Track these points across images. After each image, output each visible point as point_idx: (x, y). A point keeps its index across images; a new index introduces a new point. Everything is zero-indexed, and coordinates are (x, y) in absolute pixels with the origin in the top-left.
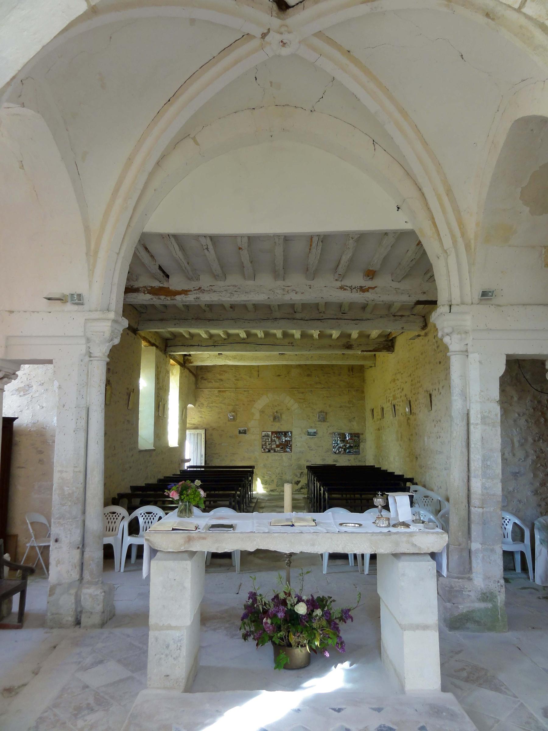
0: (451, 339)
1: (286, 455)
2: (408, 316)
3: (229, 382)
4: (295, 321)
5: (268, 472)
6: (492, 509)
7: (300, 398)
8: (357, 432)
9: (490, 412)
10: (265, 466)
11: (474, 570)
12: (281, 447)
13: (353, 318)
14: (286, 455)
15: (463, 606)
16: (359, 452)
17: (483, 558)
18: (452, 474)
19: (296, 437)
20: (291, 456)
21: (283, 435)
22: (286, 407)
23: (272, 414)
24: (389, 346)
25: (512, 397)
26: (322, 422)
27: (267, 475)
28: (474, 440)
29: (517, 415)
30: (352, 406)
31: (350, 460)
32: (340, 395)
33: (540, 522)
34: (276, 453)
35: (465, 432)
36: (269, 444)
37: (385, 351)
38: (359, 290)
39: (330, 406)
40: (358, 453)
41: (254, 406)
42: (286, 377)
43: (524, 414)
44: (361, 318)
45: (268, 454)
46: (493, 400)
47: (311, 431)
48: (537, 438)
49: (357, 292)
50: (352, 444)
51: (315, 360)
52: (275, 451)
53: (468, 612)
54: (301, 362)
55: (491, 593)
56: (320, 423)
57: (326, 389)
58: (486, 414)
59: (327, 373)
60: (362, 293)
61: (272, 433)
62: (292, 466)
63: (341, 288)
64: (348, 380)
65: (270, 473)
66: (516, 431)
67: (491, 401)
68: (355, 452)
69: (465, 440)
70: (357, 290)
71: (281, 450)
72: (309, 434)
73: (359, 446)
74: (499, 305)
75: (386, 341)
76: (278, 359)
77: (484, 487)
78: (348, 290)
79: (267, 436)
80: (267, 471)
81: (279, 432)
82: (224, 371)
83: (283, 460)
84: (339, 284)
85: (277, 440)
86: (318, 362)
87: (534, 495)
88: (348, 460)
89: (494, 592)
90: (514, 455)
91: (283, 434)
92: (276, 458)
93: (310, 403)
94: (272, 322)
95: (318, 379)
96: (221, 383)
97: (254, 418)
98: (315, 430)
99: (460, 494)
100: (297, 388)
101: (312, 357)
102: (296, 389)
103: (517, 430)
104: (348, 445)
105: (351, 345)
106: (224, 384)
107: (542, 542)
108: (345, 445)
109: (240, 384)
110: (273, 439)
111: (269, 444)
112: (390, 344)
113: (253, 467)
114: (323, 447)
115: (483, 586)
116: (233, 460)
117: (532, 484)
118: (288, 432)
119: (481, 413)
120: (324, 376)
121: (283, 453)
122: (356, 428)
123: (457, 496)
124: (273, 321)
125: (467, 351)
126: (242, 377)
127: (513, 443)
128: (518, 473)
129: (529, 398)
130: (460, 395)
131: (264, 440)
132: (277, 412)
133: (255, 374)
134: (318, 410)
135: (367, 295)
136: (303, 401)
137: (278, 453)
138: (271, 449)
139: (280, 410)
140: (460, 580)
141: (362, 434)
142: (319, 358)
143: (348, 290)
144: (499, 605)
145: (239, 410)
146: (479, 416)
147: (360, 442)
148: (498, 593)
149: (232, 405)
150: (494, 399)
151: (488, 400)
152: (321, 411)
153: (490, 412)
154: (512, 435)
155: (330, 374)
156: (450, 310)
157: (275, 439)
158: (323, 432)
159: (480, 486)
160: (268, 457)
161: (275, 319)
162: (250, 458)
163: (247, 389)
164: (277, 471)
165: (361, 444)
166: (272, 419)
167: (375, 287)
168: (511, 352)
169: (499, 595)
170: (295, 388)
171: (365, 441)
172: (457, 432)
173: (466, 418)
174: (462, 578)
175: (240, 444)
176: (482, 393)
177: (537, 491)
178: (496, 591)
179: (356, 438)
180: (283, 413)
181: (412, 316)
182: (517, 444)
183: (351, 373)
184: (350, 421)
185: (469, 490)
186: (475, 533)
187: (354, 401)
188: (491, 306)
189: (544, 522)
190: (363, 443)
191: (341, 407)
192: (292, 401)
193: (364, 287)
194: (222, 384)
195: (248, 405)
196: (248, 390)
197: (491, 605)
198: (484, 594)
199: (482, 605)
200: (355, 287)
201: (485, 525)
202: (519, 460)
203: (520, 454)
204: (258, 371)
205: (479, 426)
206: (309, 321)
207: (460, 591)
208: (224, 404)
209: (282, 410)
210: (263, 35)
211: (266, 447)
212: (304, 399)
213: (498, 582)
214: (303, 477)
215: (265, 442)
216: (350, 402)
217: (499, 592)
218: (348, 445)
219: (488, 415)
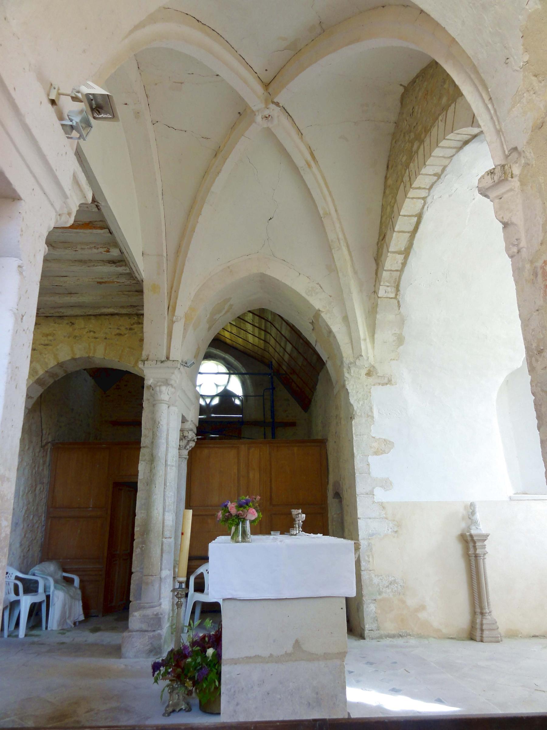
18: (157, 509)
28: (170, 479)
186: (165, 561)
210: (277, 103)
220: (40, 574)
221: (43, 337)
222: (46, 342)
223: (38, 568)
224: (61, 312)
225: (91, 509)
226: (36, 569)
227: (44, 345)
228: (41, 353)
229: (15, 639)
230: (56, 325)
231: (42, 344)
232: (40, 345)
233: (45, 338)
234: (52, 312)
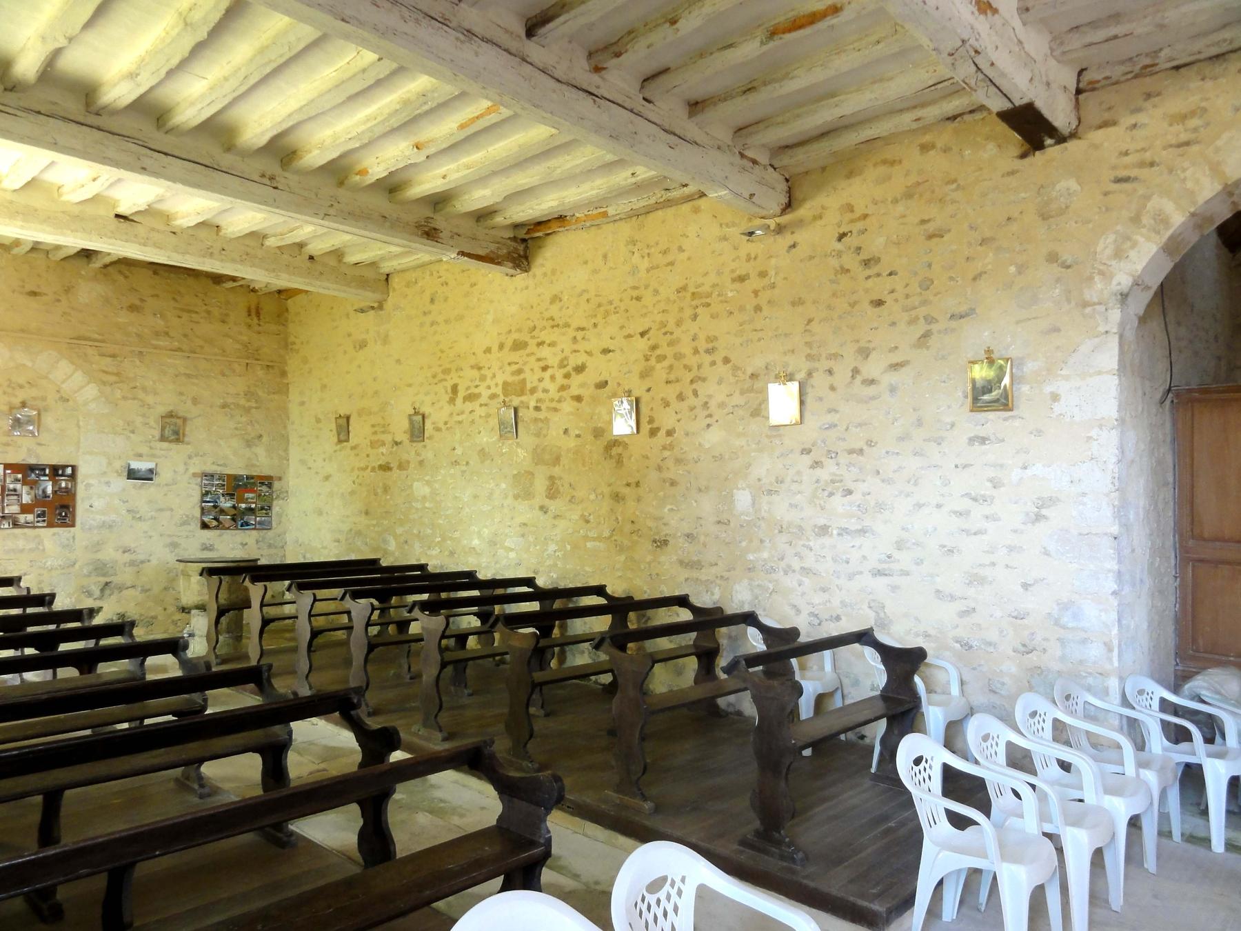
1: (54, 534)
2: (765, 167)
8: (266, 472)
12: (38, 510)
14: (54, 534)
16: (270, 523)
19: (91, 481)
20: (74, 538)
21: (45, 475)
22: (58, 391)
24: (520, 256)
26: (171, 442)
30: (254, 405)
31: (246, 544)
32: (223, 375)
34: (17, 531)
37: (511, 265)
39: (195, 401)
40: (265, 526)
42: (59, 301)
47: (141, 465)
50: (253, 503)
51: (234, 261)
52: (16, 524)
54: (188, 257)
56: (165, 445)
57: (184, 354)
59: (189, 311)
62: (77, 566)
64: (245, 338)
68: (260, 523)
71: (38, 522)
72: (132, 474)
73: (270, 508)
75: (514, 239)
76: (112, 232)
81: (32, 468)
83: (44, 550)
86: (239, 266)
88: (242, 544)
91: (47, 471)
92: (21, 543)
94: (457, 39)
95: (162, 323)
98: (151, 465)
101: (223, 250)
102: (91, 343)
104: (243, 506)
105: (435, 229)
108: (234, 507)
110: (11, 486)
112: (521, 248)
114: (172, 510)
118: (64, 467)
120: (179, 317)
121: (43, 529)
122: (262, 463)
124: (462, 37)
134: (162, 410)
136: (113, 378)
137: (26, 530)
139: (34, 398)
141: (280, 479)
147: (272, 500)
152: (172, 411)
155: (197, 312)
157: (18, 486)
158: (175, 471)
161: (468, 31)
165: (275, 503)
171: (284, 495)
179: (264, 488)
180: (46, 410)
181: (771, 170)
183: (255, 320)
184: (249, 444)
187: (260, 393)
190: (281, 502)
191: (224, 406)
192: (79, 377)
209: (44, 399)
212: (118, 374)
214: (110, 595)
216: (249, 394)
218: (243, 506)
220: (1218, 700)
221: (1171, 125)
222: (1184, 137)
223: (1205, 684)
224: (1225, 40)
226: (1199, 684)
227: (1179, 146)
228: (1171, 171)
229: (1201, 852)
230: (1209, 84)
231: (1171, 146)
232: (1165, 148)
233: (1178, 128)
234: (1199, 45)
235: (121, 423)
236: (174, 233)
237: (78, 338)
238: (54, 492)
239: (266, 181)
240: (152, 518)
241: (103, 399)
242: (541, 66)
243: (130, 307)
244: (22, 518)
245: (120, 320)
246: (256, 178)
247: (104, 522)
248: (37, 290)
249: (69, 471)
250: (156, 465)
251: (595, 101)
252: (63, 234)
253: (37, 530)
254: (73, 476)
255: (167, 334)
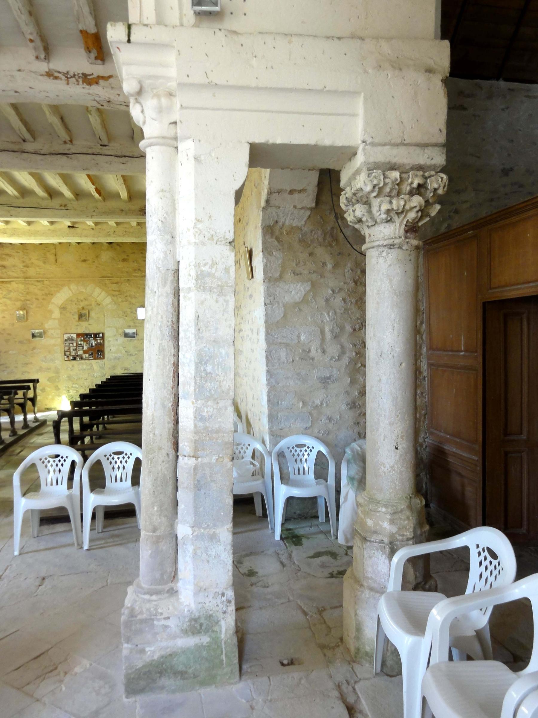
0: (142, 111)
1: (97, 363)
3: (15, 269)
4: (25, 155)
5: (74, 386)
6: (214, 458)
7: (114, 289)
9: (214, 264)
10: (69, 378)
11: (181, 575)
12: (90, 353)
13: (119, 154)
14: (97, 363)
15: (153, 649)
17: (195, 554)
19: (110, 339)
22: (96, 301)
23: (76, 311)
25: (324, 264)
27: (73, 389)
29: (330, 291)
33: (352, 450)
34: (83, 361)
35: (170, 306)
36: (74, 350)
38: (81, 80)
41: (53, 301)
43: (341, 289)
44: (131, 155)
45: (74, 362)
46: (222, 239)
48: (357, 327)
49: (78, 84)
51: (119, 236)
52: (82, 359)
53: (162, 657)
54: (99, 238)
55: (209, 617)
58: (203, 268)
60: (88, 87)
61: (78, 335)
63: (49, 74)
65: (77, 386)
66: (329, 315)
67: (218, 240)
69: (170, 323)
70: (77, 81)
72: (126, 335)
74: (235, 32)
76: (67, 234)
77: (199, 416)
78: (61, 79)
79: (72, 339)
80: (73, 384)
81: (87, 335)
82: (7, 255)
84: (43, 67)
85: (84, 344)
87: (351, 408)
89: (214, 615)
90: (324, 352)
92: (85, 366)
93: (127, 296)
95: (136, 264)
96: (4, 270)
97: (53, 317)
98: (134, 331)
99: (157, 432)
100: (109, 277)
103: (330, 314)
106: (8, 272)
107: (351, 479)
109: (31, 272)
110: (80, 343)
111: (74, 350)
113: (36, 381)
115: (193, 606)
116: (26, 372)
117: (347, 393)
118: (99, 334)
119: (197, 266)
123: (151, 435)
125: (176, 139)
126: (33, 263)
127: (323, 333)
128: (329, 378)
129: (349, 265)
130: (160, 230)
131: (67, 344)
132: (83, 308)
133: (52, 258)
135: (95, 89)
136: (117, 293)
137: (86, 361)
138: (77, 356)
139: (87, 305)
140: (154, 597)
142: (124, 233)
143: (61, 79)
144: (223, 636)
145: (31, 306)
146: (193, 273)
148: (222, 616)
149: (21, 301)
150: (224, 237)
151: (212, 238)
153: (214, 264)
154: (322, 322)
156: (129, 36)
157: (82, 343)
159: (192, 416)
160: (73, 366)
162: (49, 369)
163: (41, 278)
164: (85, 383)
166: (76, 317)
167: (110, 77)
168: (259, 139)
169: (223, 618)
170: (107, 277)
172: (152, 309)
173: (170, 278)
174: (157, 593)
175: (34, 351)
176: (200, 226)
177: (354, 403)
178: (218, 611)
180: (91, 310)
182: (328, 335)
185: (177, 422)
188: (217, 31)
189: (359, 449)
192: (103, 294)
193: (90, 75)
194: (6, 272)
195: (44, 299)
196: (42, 279)
197: (208, 639)
198: (196, 620)
199: (191, 641)
200: (74, 75)
201: (199, 490)
202: (331, 359)
203: (333, 350)
204: (56, 255)
205: (192, 295)
206: (48, 156)
207: (149, 621)
208: (10, 299)
209: (90, 305)
211: (70, 354)
212: (119, 291)
213: (223, 595)
215: (67, 348)
217: (225, 613)
219: (209, 270)
225: (462, 353)
235: (121, 312)
236: (93, 229)
237: (103, 277)
238: (96, 344)
239: (63, 208)
240: (136, 354)
241: (114, 303)
242: (33, 151)
243: (123, 260)
244: (85, 356)
245: (119, 266)
246: (58, 207)
247: (116, 357)
248: (85, 259)
249: (101, 335)
250: (136, 330)
251: (68, 157)
252: (60, 239)
253: (90, 361)
254: (103, 338)
255: (139, 270)
